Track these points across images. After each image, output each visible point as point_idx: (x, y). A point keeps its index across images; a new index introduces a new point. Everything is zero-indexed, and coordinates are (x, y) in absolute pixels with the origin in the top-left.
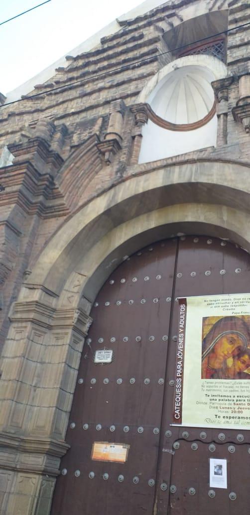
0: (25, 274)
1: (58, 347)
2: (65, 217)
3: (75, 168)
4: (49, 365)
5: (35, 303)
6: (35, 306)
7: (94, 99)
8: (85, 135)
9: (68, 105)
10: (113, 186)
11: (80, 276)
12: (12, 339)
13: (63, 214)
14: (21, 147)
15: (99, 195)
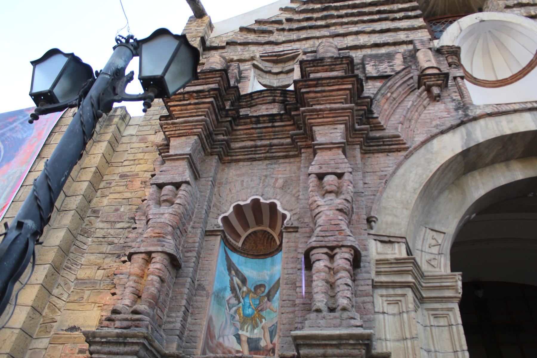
0: (369, 221)
1: (443, 328)
2: (404, 153)
3: (392, 98)
4: (438, 354)
5: (413, 261)
6: (412, 265)
7: (353, 41)
8: (384, 68)
9: (314, 42)
10: (462, 123)
11: (434, 233)
12: (384, 313)
13: (398, 148)
14: (321, 63)
15: (442, 132)
